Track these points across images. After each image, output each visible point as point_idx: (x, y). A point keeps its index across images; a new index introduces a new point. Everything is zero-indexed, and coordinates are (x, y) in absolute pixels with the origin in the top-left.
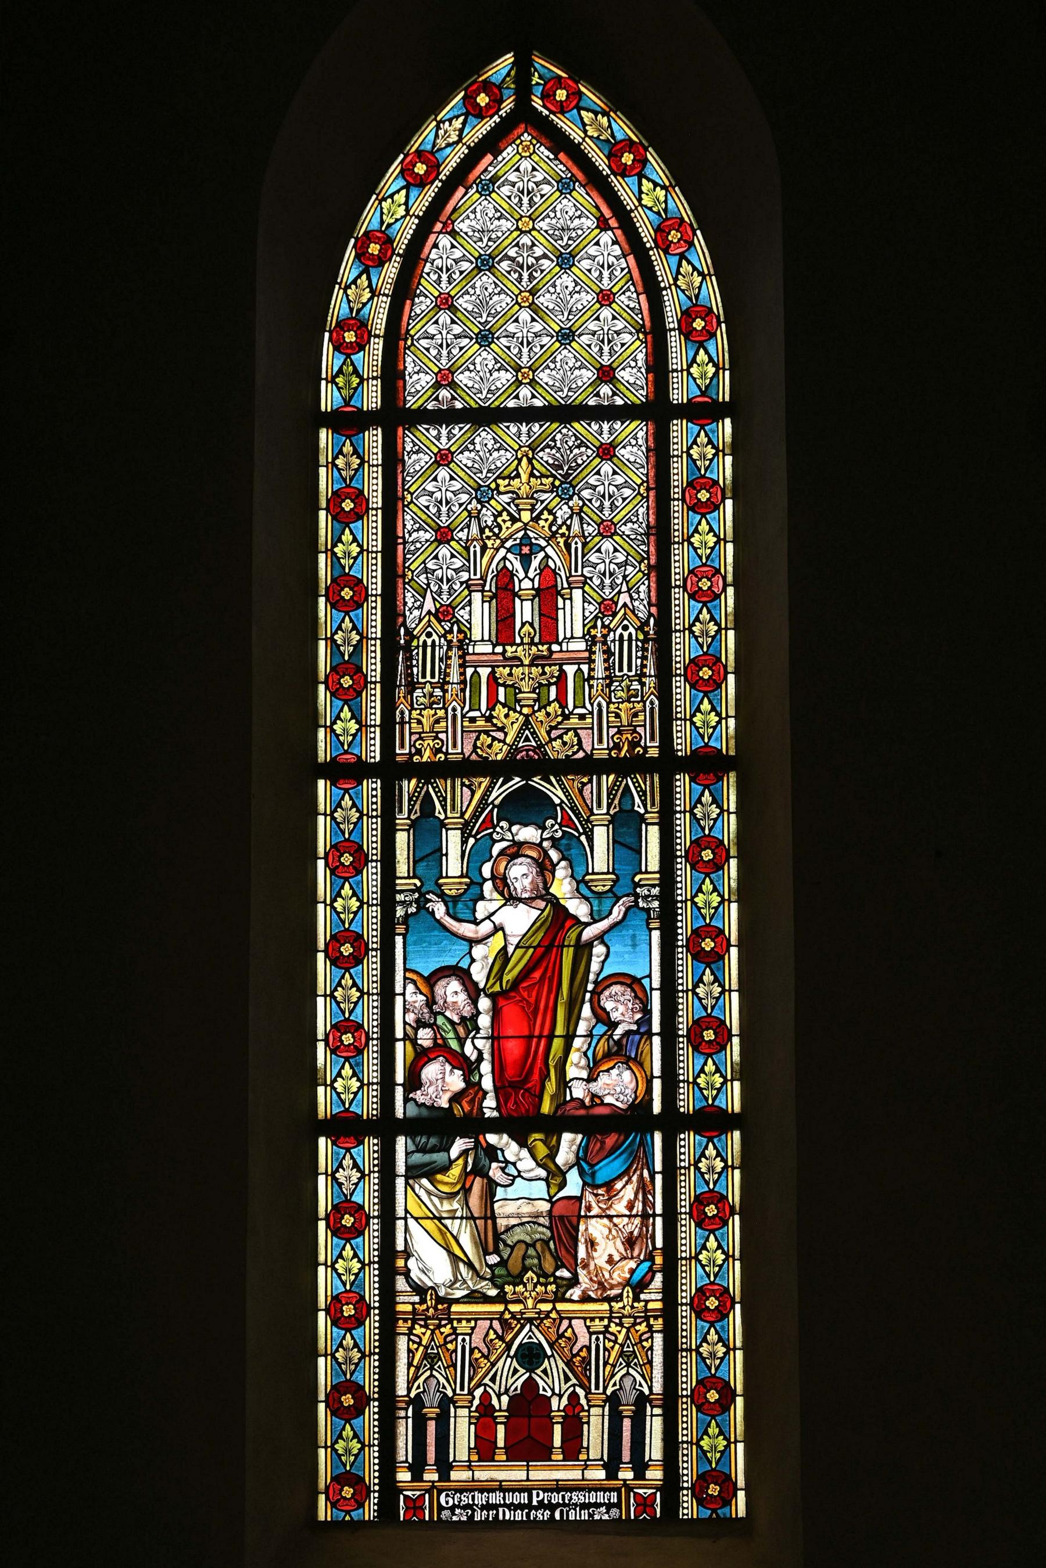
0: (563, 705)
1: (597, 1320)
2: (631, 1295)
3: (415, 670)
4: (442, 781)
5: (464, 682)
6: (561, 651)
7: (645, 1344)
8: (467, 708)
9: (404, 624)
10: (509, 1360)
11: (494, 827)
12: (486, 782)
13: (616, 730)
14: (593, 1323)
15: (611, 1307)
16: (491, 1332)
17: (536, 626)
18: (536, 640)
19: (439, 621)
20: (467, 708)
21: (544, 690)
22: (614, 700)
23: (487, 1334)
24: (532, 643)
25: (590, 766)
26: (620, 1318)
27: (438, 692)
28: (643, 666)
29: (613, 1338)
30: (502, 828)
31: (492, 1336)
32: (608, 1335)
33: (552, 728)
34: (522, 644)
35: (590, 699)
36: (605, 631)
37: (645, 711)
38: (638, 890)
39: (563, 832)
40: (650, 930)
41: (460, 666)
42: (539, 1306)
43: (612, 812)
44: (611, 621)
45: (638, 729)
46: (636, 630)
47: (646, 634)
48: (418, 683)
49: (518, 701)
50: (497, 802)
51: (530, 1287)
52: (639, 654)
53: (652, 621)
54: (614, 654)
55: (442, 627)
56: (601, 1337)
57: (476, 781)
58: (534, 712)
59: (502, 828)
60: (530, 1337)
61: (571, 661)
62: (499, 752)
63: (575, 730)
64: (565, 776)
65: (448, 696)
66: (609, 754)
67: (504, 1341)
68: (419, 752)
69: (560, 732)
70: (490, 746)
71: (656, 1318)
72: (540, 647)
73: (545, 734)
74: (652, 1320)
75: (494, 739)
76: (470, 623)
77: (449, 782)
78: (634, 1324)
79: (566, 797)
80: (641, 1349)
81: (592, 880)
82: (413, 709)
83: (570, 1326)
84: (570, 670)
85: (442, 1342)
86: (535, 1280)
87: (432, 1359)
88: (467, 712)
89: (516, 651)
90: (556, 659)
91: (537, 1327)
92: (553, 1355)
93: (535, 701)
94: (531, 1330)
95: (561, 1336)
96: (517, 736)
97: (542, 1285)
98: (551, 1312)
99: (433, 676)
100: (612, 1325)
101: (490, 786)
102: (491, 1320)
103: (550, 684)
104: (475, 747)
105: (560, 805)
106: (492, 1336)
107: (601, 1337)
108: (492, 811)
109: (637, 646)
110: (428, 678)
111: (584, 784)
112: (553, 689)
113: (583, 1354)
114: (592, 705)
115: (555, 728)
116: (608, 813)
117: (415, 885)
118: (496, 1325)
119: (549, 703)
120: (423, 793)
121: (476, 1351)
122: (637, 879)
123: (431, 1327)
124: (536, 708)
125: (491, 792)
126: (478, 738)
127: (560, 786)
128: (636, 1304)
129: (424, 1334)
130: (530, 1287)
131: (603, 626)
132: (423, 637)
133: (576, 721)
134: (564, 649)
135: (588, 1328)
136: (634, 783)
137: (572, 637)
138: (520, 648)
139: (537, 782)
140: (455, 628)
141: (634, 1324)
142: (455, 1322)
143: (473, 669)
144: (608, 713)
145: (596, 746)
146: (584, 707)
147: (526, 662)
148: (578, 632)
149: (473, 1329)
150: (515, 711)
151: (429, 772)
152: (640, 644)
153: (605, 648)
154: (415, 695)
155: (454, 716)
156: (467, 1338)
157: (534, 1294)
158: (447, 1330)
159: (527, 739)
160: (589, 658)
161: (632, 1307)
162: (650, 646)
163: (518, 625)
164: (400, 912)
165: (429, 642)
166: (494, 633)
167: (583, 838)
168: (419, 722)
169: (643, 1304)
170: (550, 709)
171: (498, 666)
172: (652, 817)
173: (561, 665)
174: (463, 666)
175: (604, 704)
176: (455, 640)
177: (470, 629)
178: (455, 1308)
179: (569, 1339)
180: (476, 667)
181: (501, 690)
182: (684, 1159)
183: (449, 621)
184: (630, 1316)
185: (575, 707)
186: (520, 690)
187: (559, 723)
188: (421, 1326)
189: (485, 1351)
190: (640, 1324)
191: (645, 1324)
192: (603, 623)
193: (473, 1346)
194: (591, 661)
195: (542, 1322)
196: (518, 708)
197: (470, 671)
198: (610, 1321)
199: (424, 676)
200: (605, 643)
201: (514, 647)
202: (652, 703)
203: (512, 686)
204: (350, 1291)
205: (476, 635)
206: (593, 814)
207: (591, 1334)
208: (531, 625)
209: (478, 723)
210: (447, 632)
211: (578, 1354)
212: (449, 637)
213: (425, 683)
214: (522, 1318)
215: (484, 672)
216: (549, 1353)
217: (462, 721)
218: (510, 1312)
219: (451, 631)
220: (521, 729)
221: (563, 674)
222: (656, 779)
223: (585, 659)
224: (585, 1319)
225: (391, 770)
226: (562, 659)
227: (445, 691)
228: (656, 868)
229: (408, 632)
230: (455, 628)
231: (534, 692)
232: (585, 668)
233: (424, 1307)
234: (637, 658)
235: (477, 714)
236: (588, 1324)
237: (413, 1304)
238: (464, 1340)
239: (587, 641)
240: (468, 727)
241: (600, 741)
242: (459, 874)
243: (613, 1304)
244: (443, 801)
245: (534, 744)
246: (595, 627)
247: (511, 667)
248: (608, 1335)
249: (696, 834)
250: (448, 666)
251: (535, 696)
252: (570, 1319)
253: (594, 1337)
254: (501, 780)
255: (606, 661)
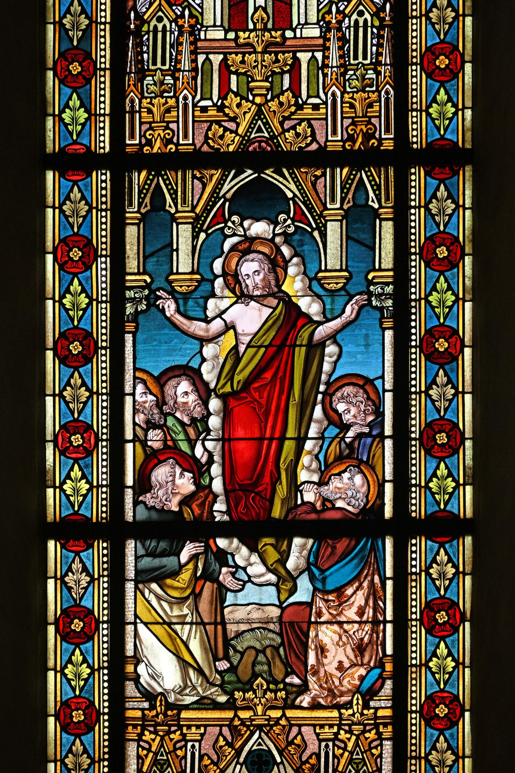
0: (297, 95)
1: (327, 727)
2: (360, 702)
3: (145, 56)
4: (173, 174)
5: (195, 70)
6: (295, 37)
7: (374, 751)
8: (198, 97)
9: (134, 8)
10: (238, 767)
11: (226, 222)
12: (217, 174)
13: (350, 121)
14: (322, 731)
15: (341, 714)
16: (221, 739)
17: (270, 10)
18: (270, 25)
19: (170, 6)
20: (198, 97)
21: (277, 78)
22: (348, 90)
23: (217, 741)
24: (265, 29)
25: (324, 159)
26: (350, 725)
27: (169, 80)
28: (379, 54)
29: (342, 745)
30: (233, 222)
31: (222, 742)
32: (337, 743)
33: (285, 118)
34: (255, 29)
35: (324, 88)
36: (340, 17)
37: (380, 102)
38: (372, 288)
39: (296, 227)
40: (384, 330)
41: (192, 52)
42: (269, 713)
43: (345, 207)
44: (346, 7)
45: (373, 120)
46: (372, 16)
47: (382, 20)
48: (149, 70)
49: (250, 90)
50: (228, 196)
51: (259, 693)
52: (374, 42)
53: (388, 6)
54: (349, 41)
55: (173, 11)
56: (331, 744)
57: (207, 173)
58: (267, 101)
59: (233, 222)
60: (260, 744)
61: (305, 49)
62: (231, 144)
63: (309, 120)
64: (298, 168)
65: (180, 84)
66: (343, 146)
67: (233, 748)
68: (149, 143)
69: (293, 123)
70: (222, 137)
71: (385, 725)
72: (273, 33)
73: (278, 125)
74: (381, 727)
75: (226, 129)
76: (202, 8)
77: (180, 174)
78: (364, 732)
79: (299, 190)
80: (370, 757)
81: (325, 278)
82: (143, 97)
83: (300, 733)
84: (304, 57)
85: (171, 749)
86: (265, 687)
87: (162, 765)
88: (199, 101)
89: (249, 37)
90: (290, 46)
91: (267, 734)
92: (282, 762)
93: (268, 90)
94: (260, 737)
95: (291, 743)
96: (250, 127)
97: (271, 691)
98: (280, 718)
99: (163, 63)
100: (342, 732)
101: (221, 179)
102: (221, 726)
103: (283, 73)
104: (207, 137)
105: (293, 199)
106: (222, 742)
107: (331, 744)
108: (223, 205)
109: (372, 33)
110: (159, 65)
111: (317, 178)
112: (287, 78)
113: (313, 761)
114: (326, 94)
115: (288, 118)
116: (341, 208)
117: (145, 281)
118: (226, 731)
119: (282, 93)
120: (153, 185)
121: (206, 758)
122: (370, 277)
123: (161, 733)
124: (269, 97)
125: (223, 185)
126: (209, 129)
127: (293, 179)
128: (365, 712)
129: (153, 740)
130: (259, 693)
131: (338, 11)
132: (154, 22)
133: (310, 111)
134: (298, 35)
135: (318, 735)
136: (368, 177)
137: (306, 23)
138: (253, 34)
139: (269, 175)
140: (187, 12)
141: (364, 732)
142: (185, 729)
143: (204, 56)
144: (342, 102)
145: (330, 138)
146: (318, 96)
147: (259, 49)
148: (313, 18)
149: (202, 735)
150: (247, 100)
151: (159, 164)
152: (375, 30)
153: (340, 35)
154: (145, 82)
155: (186, 106)
156: (197, 744)
157: (263, 700)
158: (176, 736)
159: (260, 130)
160: (324, 45)
161: (362, 714)
162: (385, 33)
163: (251, 10)
164: (129, 309)
165: (160, 27)
166: (226, 18)
167: (316, 234)
168: (150, 111)
169: (372, 711)
170: (283, 99)
171: (230, 53)
172: (386, 212)
173: (294, 53)
174: (195, 53)
175: (338, 93)
176: (186, 25)
177: (202, 14)
178: (184, 715)
179: (299, 746)
180: (207, 54)
181: (234, 78)
182: (415, 565)
183: (180, 5)
184: (359, 724)
185: (309, 96)
186: (252, 78)
187: (292, 114)
188: (151, 732)
189: (215, 758)
190: (369, 731)
191: (374, 732)
192: (338, 8)
193: (203, 752)
194: (325, 49)
195: (271, 728)
196: (251, 98)
197: (201, 58)
198: (339, 729)
199: (155, 63)
200: (339, 29)
201: (247, 33)
202: (387, 93)
203: (245, 74)
204: (79, 696)
205: (208, 20)
206: (326, 209)
207: (320, 741)
208: (265, 9)
209: (210, 113)
210: (178, 17)
211: (307, 761)
212: (180, 22)
213: (156, 70)
214: (252, 725)
215: (216, 59)
216: (279, 760)
217: (193, 111)
218: (240, 719)
219: (182, 16)
220: (254, 119)
221: (297, 62)
222: (391, 173)
223: (319, 46)
224: (314, 726)
225: (120, 162)
226: (296, 46)
227: (176, 79)
228: (391, 266)
229: (139, 17)
230: (187, 12)
231: (266, 80)
232: (319, 55)
233: (154, 713)
234: (372, 45)
235: (208, 103)
236: (318, 731)
237: (143, 710)
238: (193, 747)
239: (321, 27)
240: (200, 117)
241: (334, 133)
242: (190, 270)
243: (343, 711)
244: (174, 194)
245: (266, 135)
246: (330, 12)
247: (244, 54)
248: (337, 743)
249: (431, 230)
250: (179, 53)
251: (268, 84)
252: (300, 726)
253: (323, 744)
254: (233, 172)
255: (341, 48)
